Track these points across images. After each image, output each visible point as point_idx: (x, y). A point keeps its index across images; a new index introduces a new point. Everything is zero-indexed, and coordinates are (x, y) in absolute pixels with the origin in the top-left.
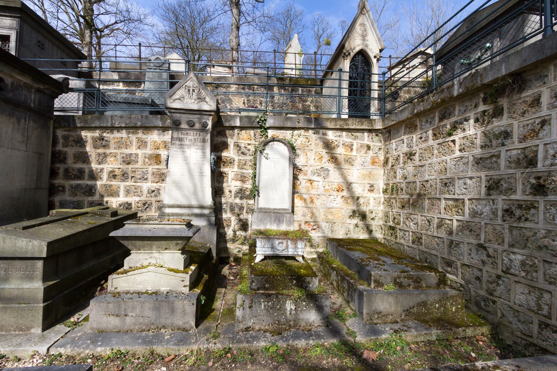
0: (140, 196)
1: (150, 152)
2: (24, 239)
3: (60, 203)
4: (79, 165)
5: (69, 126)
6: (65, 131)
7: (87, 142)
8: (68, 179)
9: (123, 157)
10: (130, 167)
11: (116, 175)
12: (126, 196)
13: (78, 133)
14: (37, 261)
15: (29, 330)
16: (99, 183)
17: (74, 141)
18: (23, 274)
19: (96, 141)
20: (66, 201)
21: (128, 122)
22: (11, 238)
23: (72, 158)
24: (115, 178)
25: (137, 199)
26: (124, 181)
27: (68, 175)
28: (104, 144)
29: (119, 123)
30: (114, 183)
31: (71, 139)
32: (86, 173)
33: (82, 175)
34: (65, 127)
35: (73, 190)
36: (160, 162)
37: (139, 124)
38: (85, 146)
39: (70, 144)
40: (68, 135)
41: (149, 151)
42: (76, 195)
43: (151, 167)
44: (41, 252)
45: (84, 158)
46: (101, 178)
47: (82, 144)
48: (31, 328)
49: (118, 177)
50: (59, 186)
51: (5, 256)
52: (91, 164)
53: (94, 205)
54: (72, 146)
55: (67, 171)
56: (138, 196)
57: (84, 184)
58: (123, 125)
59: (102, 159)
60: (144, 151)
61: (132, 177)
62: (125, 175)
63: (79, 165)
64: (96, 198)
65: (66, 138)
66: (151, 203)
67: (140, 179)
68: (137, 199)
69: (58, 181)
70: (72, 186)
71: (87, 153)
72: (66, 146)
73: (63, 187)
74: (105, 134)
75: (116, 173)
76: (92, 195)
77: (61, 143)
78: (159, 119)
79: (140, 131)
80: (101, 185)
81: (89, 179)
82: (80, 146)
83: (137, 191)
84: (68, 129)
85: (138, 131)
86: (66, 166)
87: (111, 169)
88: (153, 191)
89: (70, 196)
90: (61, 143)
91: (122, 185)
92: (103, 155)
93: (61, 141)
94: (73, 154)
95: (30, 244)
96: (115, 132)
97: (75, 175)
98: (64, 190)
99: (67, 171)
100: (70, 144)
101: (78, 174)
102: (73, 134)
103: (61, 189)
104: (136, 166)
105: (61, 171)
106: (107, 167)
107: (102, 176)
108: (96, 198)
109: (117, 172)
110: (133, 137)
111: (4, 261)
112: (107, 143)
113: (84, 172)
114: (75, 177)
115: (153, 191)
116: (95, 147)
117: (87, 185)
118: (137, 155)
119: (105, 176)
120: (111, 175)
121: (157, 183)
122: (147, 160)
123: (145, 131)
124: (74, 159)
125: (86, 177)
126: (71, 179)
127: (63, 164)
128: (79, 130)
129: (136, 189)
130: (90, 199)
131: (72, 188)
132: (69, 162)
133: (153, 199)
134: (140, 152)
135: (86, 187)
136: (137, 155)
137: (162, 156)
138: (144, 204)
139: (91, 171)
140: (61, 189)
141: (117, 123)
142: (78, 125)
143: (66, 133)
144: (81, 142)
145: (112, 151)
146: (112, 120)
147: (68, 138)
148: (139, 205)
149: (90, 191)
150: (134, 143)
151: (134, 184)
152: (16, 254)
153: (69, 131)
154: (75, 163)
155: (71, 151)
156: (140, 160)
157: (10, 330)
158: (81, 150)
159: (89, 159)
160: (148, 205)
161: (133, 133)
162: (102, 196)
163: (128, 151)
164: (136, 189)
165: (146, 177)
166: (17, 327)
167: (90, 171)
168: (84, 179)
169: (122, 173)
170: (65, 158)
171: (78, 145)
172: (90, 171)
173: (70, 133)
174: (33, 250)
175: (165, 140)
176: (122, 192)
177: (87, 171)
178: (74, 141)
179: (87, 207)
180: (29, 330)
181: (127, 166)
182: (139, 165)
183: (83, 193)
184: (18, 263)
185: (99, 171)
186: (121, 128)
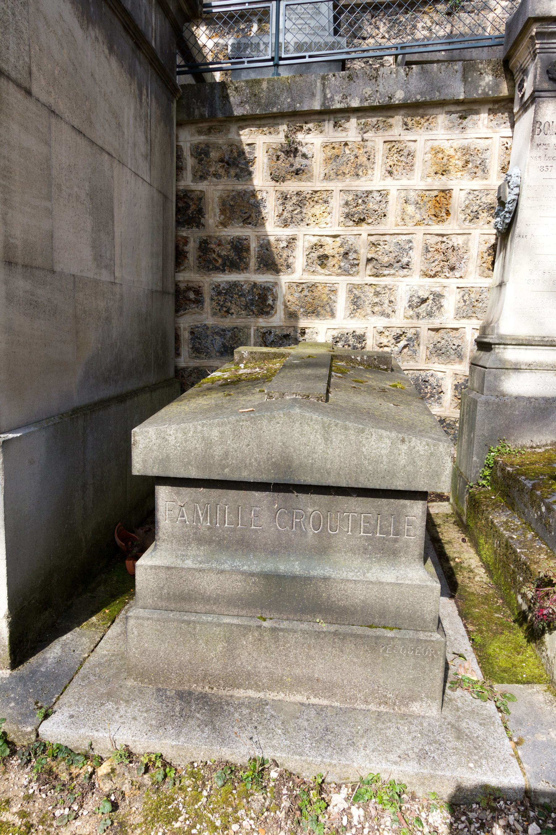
0: (388, 316)
1: (422, 185)
2: (385, 433)
3: (192, 333)
4: (235, 231)
5: (213, 116)
6: (200, 133)
7: (253, 161)
8: (209, 270)
9: (347, 204)
10: (364, 229)
11: (326, 257)
12: (352, 314)
13: (232, 136)
14: (407, 502)
15: (407, 705)
16: (285, 279)
17: (221, 160)
18: (368, 539)
19: (278, 157)
20: (206, 327)
21: (368, 91)
22: (346, 428)
23: (217, 211)
24: (323, 265)
25: (381, 322)
26: (346, 273)
27: (208, 259)
28: (297, 166)
29: (345, 97)
30: (321, 277)
31: (214, 155)
32: (252, 252)
33: (241, 259)
34: (202, 119)
35: (222, 298)
36: (448, 213)
37: (399, 96)
38: (250, 174)
39: (212, 169)
40: (207, 145)
41: (419, 180)
42: (227, 312)
43: (422, 229)
44: (437, 475)
45: (246, 208)
46: (288, 266)
47: (242, 170)
48: (413, 699)
49: (331, 262)
50: (189, 289)
51: (331, 481)
52: (263, 225)
53: (271, 338)
54: (216, 175)
55: (204, 246)
56: (383, 314)
57: (246, 282)
58: (355, 104)
59: (297, 208)
60: (404, 182)
61: (369, 260)
62: (352, 256)
63: (235, 231)
64: (277, 319)
65: (201, 153)
66: (417, 335)
67: (390, 265)
68: (381, 322)
69: (189, 276)
70: (217, 289)
71: (253, 194)
72: (203, 178)
73: (198, 292)
74: (300, 137)
75: (328, 251)
76: (268, 313)
77: (189, 168)
78: (459, 76)
79: (397, 120)
80: (290, 285)
81: (258, 270)
82: (237, 176)
83: (382, 305)
84: (205, 125)
85: (390, 120)
86: (200, 234)
87: (314, 240)
88: (424, 301)
89: (214, 314)
90: (189, 168)
91: (342, 283)
92: (295, 199)
93: (190, 162)
94: (220, 197)
95: (404, 447)
96: (328, 126)
97: (226, 259)
98: (199, 302)
99: (204, 246)
100: (212, 169)
101: (233, 254)
102: (220, 140)
103: (192, 296)
104: (381, 229)
105: (192, 248)
106: (305, 236)
107: (291, 260)
108: (277, 319)
109: (331, 247)
110: (377, 141)
111: (316, 497)
112: (304, 162)
113: (248, 250)
114: (224, 265)
115: (424, 301)
116: (276, 178)
117: (255, 285)
118: (383, 194)
119: (299, 259)
120: (315, 255)
121: (434, 276)
122: (411, 209)
123: (408, 120)
124: (223, 211)
125: (253, 262)
126: (217, 269)
127: (195, 229)
128: (233, 128)
129: (377, 294)
130: (262, 322)
131: (219, 293)
132: (211, 221)
133: (424, 325)
134: (392, 186)
135: (251, 291)
136: (383, 194)
137: (455, 194)
138: (397, 338)
139: (266, 247)
140: (192, 296)
141: (337, 98)
142: (238, 112)
143: (202, 138)
144: (238, 163)
145: (319, 185)
146: (324, 90)
147: (207, 154)
148: (385, 341)
149: (261, 301)
150: (379, 159)
151: (373, 280)
152: (361, 479)
153: (209, 131)
154: (224, 224)
155: (213, 191)
156: (393, 208)
157: (354, 698)
158: (240, 187)
159: (260, 212)
160: (410, 339)
161: (377, 128)
162: (292, 316)
163: (361, 185)
164: (377, 294)
165: (405, 260)
166: (372, 693)
167: (261, 246)
168: (246, 268)
169: (342, 251)
170: (200, 212)
171: (233, 172)
172: (261, 246)
173: (213, 139)
174: (409, 468)
175: (465, 143)
176: (341, 302)
177: (253, 245)
178: (221, 160)
179: (255, 345)
180: (407, 705)
181: (356, 230)
182: (390, 224)
183: (246, 307)
184: (353, 502)
185: (284, 244)
186: (348, 112)
